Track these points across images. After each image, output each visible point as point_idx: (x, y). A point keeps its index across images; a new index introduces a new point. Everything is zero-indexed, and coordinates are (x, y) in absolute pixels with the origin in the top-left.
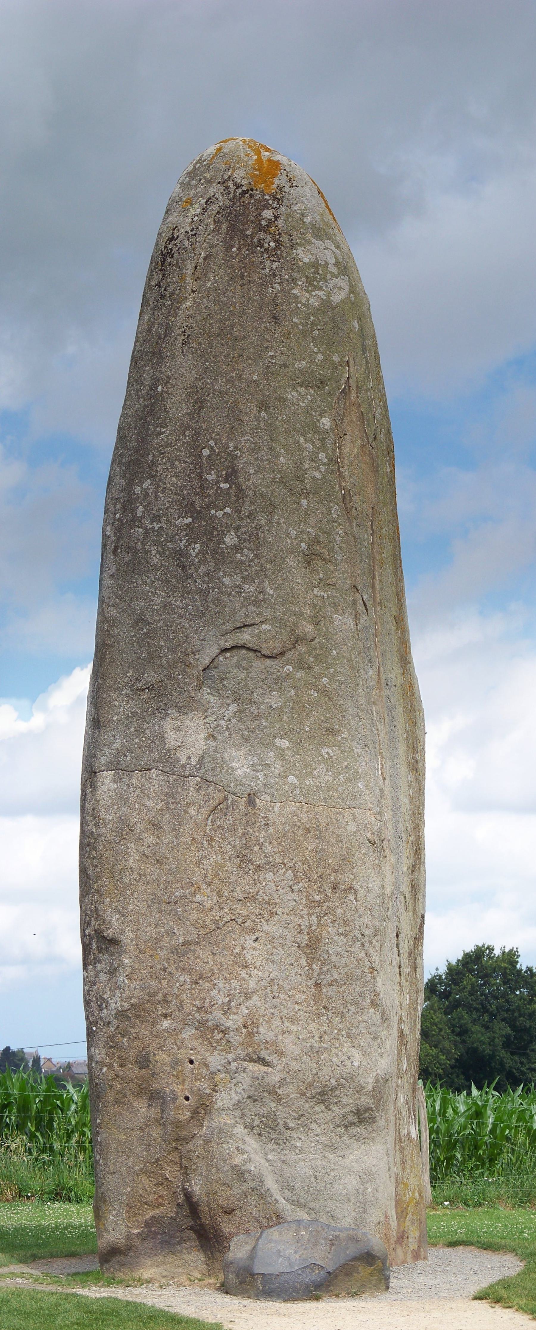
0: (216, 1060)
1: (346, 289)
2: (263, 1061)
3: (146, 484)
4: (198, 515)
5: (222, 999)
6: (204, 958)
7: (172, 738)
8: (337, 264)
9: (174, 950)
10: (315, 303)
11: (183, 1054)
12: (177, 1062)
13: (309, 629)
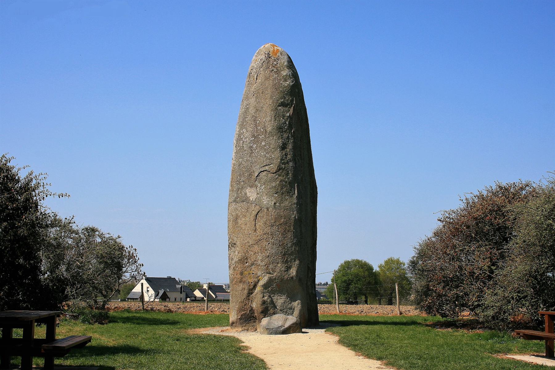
2: (270, 273)
4: (255, 137)
9: (249, 246)
10: (286, 85)
11: (251, 272)
12: (249, 274)
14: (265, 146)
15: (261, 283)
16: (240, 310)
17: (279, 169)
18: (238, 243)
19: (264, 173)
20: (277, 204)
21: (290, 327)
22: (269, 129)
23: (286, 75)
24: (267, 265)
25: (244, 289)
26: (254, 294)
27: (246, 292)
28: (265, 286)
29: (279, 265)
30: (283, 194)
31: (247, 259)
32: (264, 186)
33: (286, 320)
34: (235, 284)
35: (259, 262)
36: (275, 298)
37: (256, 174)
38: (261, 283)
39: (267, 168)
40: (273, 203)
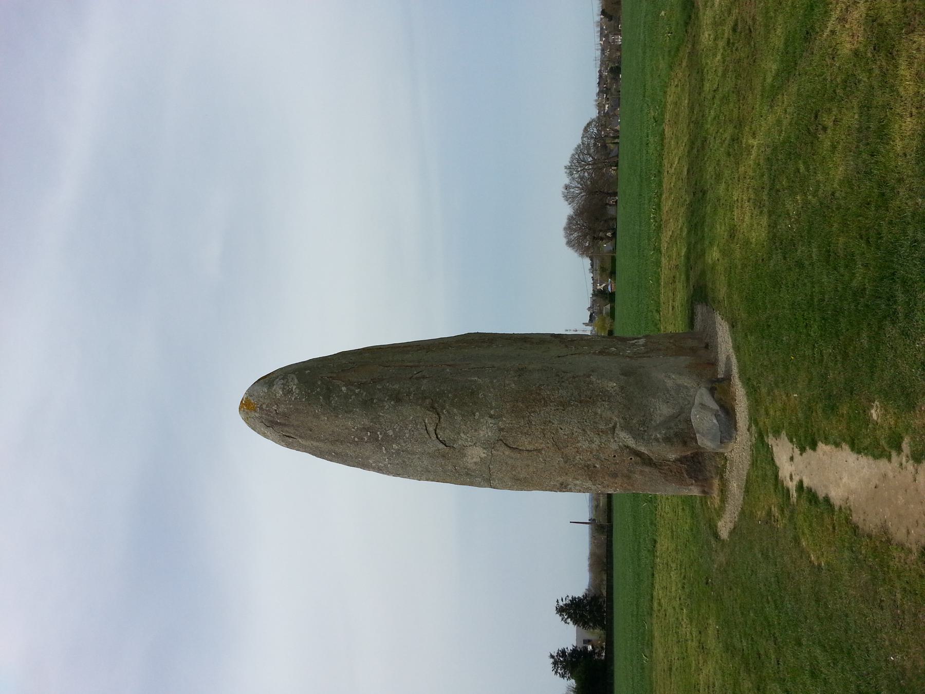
0: (614, 446)
1: (293, 376)
2: (614, 428)
3: (371, 461)
6: (570, 451)
7: (474, 460)
8: (283, 379)
9: (566, 462)
13: (428, 401)
14: (394, 430)
16: (681, 482)
17: (432, 408)
18: (560, 479)
20: (492, 412)
22: (366, 422)
23: (283, 389)
24: (599, 433)
25: (641, 471)
26: (651, 455)
27: (647, 469)
28: (637, 435)
29: (599, 411)
30: (475, 403)
31: (588, 467)
32: (462, 435)
33: (703, 406)
35: (593, 446)
36: (658, 420)
37: (441, 446)
38: (631, 442)
39: (431, 429)
40: (490, 421)
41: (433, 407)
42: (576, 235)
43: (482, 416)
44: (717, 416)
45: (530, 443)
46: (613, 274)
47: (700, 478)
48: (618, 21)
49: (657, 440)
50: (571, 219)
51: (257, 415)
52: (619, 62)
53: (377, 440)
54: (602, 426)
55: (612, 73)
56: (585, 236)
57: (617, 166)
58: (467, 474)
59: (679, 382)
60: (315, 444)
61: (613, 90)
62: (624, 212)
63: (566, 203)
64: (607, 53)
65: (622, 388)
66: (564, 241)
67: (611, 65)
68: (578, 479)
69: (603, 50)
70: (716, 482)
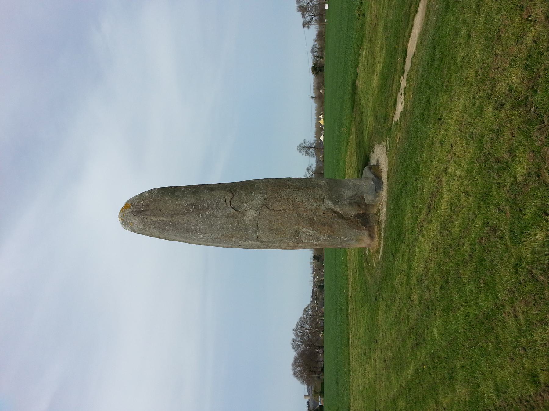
0: (324, 208)
2: (324, 199)
5: (310, 206)
6: (301, 210)
9: (299, 217)
15: (332, 206)
18: (295, 228)
19: (233, 204)
21: (374, 174)
22: (193, 200)
24: (316, 200)
27: (340, 221)
28: (335, 203)
31: (310, 219)
32: (244, 204)
34: (333, 232)
35: (313, 207)
37: (233, 210)
38: (332, 206)
40: (260, 195)
41: (230, 191)
42: (299, 369)
43: (256, 194)
44: (373, 180)
45: (280, 206)
46: (322, 393)
47: (368, 225)
48: (322, 262)
49: (345, 204)
50: (296, 359)
51: (130, 210)
52: (323, 283)
53: (197, 210)
54: (317, 198)
55: (319, 288)
56: (304, 370)
57: (323, 331)
58: (245, 228)
59: (355, 182)
60: (161, 218)
61: (320, 298)
62: (328, 359)
63: (293, 350)
64: (317, 279)
65: (327, 183)
66: (292, 372)
67: (318, 284)
68: (304, 227)
69: (314, 278)
70: (376, 227)
